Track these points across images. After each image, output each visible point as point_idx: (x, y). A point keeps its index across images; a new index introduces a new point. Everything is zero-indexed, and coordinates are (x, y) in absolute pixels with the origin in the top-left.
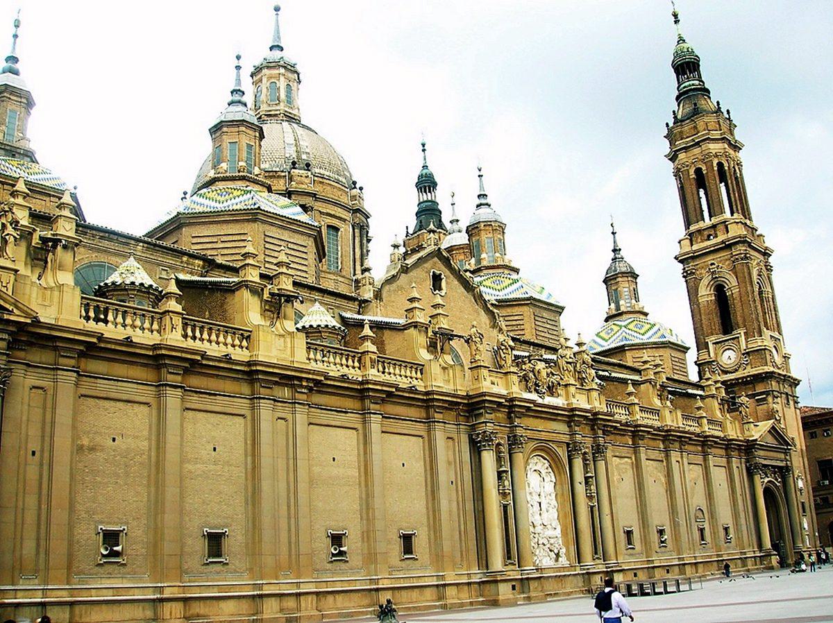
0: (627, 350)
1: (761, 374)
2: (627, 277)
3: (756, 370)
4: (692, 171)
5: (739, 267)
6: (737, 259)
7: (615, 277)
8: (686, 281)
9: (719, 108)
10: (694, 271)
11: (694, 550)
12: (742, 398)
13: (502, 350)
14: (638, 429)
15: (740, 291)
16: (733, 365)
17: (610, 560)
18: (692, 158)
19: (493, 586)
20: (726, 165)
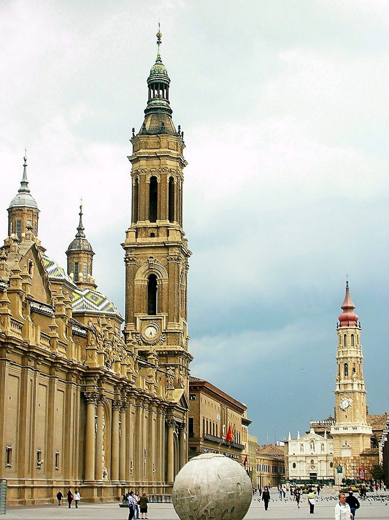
0: (86, 316)
1: (174, 351)
2: (88, 254)
3: (171, 348)
4: (148, 178)
5: (172, 266)
6: (172, 259)
7: (79, 252)
8: (127, 265)
9: (179, 131)
10: (135, 259)
11: (32, 474)
12: (169, 370)
13: (99, 337)
14: (143, 395)
15: (168, 284)
16: (153, 340)
17: (122, 480)
18: (151, 167)
19: (89, 490)
20: (175, 180)
